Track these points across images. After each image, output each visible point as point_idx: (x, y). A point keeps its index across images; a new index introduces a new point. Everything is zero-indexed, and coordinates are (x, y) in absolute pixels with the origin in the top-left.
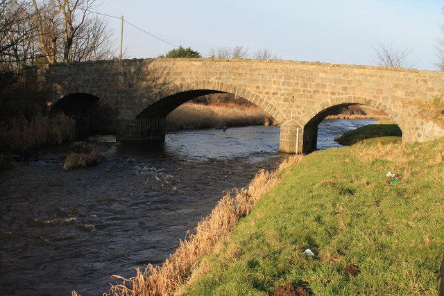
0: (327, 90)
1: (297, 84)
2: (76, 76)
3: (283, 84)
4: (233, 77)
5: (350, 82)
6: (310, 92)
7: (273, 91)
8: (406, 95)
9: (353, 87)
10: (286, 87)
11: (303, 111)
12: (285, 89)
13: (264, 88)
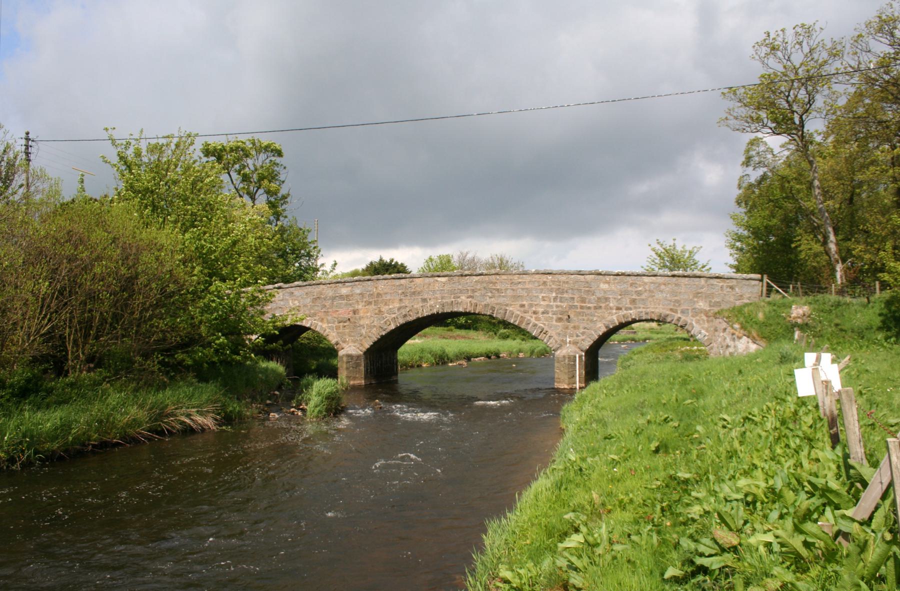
0: (611, 305)
1: (573, 298)
2: (282, 303)
3: (555, 299)
4: (490, 294)
5: (639, 293)
6: (589, 308)
7: (541, 310)
8: (710, 306)
9: (643, 300)
10: (559, 304)
11: (583, 333)
12: (557, 306)
13: (531, 305)
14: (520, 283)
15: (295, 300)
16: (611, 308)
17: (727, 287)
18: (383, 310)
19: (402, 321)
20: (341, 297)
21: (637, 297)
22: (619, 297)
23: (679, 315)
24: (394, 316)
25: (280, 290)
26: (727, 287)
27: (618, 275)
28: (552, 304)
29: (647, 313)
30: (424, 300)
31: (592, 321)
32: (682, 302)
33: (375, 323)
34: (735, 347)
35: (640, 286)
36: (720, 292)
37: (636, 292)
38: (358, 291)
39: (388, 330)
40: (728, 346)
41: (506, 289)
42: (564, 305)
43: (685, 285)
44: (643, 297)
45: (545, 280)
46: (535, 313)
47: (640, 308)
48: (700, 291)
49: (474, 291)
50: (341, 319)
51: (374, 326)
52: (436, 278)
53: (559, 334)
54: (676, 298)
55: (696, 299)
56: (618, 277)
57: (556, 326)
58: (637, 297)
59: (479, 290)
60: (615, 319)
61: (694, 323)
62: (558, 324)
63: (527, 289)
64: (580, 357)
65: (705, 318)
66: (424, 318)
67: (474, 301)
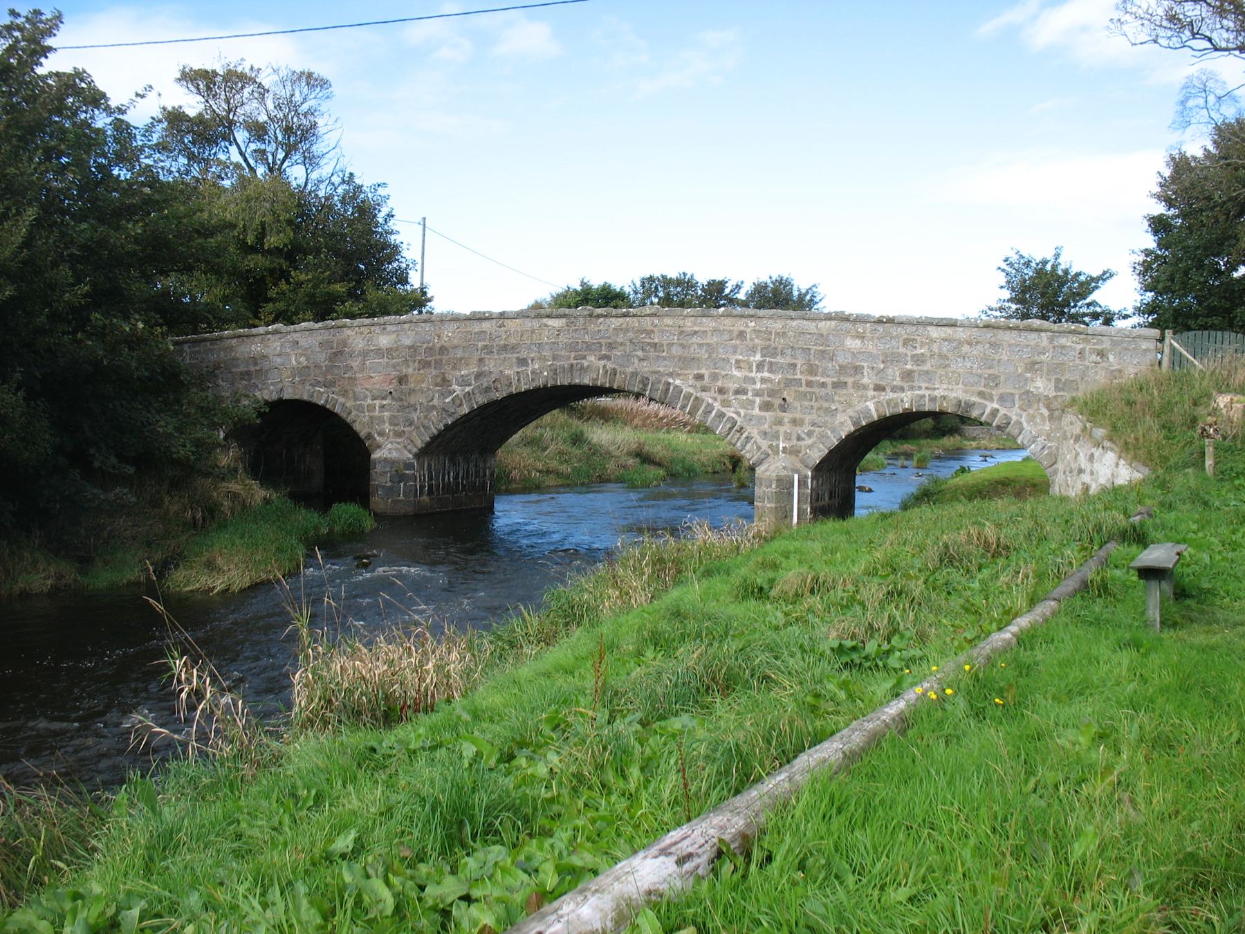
0: (866, 380)
1: (794, 366)
2: (279, 360)
3: (760, 366)
4: (640, 353)
5: (919, 360)
6: (823, 385)
7: (733, 386)
8: (1057, 388)
9: (927, 372)
10: (766, 374)
11: (810, 434)
12: (763, 380)
13: (714, 377)
14: (696, 332)
15: (301, 355)
16: (865, 388)
17: (1092, 351)
18: (449, 377)
19: (481, 400)
20: (379, 352)
21: (915, 368)
22: (882, 366)
23: (996, 406)
24: (467, 389)
25: (278, 336)
26: (1092, 351)
27: (880, 321)
28: (753, 375)
29: (933, 399)
30: (522, 362)
31: (827, 410)
32: (1002, 379)
33: (435, 402)
34: (1092, 473)
35: (922, 345)
36: (1077, 362)
37: (913, 356)
38: (408, 342)
39: (457, 416)
40: (1081, 471)
41: (671, 345)
42: (777, 377)
43: (1010, 346)
44: (927, 367)
45: (743, 328)
46: (721, 391)
47: (920, 388)
48: (1037, 358)
49: (610, 346)
50: (377, 394)
51: (434, 407)
52: (545, 320)
53: (765, 433)
54: (991, 372)
55: (1029, 375)
56: (880, 328)
57: (760, 419)
58: (915, 368)
59: (621, 344)
60: (872, 408)
61: (1023, 420)
62: (763, 414)
63: (709, 345)
64: (802, 483)
65: (1045, 412)
66: (520, 394)
67: (610, 365)
